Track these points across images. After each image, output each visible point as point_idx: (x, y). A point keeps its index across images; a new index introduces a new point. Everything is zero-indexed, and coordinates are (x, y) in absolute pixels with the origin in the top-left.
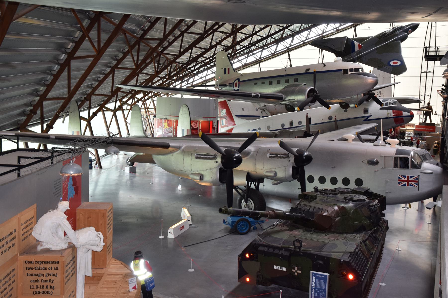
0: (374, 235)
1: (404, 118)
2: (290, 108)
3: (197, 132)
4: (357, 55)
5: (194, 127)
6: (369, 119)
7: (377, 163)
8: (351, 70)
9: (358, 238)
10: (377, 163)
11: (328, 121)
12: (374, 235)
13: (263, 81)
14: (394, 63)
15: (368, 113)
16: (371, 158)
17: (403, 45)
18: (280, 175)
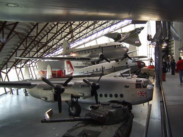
0: (126, 123)
2: (93, 63)
7: (129, 86)
8: (117, 45)
9: (119, 125)
10: (129, 86)
11: (112, 68)
12: (126, 123)
13: (82, 52)
16: (126, 85)
17: (139, 35)
18: (86, 94)
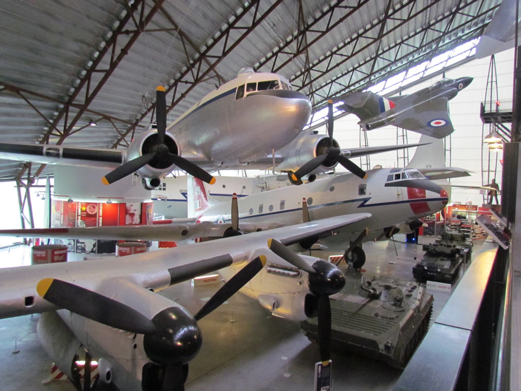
1: (429, 203)
3: (95, 221)
4: (388, 115)
5: (90, 213)
6: (367, 203)
8: (251, 86)
14: (436, 123)
17: (452, 104)
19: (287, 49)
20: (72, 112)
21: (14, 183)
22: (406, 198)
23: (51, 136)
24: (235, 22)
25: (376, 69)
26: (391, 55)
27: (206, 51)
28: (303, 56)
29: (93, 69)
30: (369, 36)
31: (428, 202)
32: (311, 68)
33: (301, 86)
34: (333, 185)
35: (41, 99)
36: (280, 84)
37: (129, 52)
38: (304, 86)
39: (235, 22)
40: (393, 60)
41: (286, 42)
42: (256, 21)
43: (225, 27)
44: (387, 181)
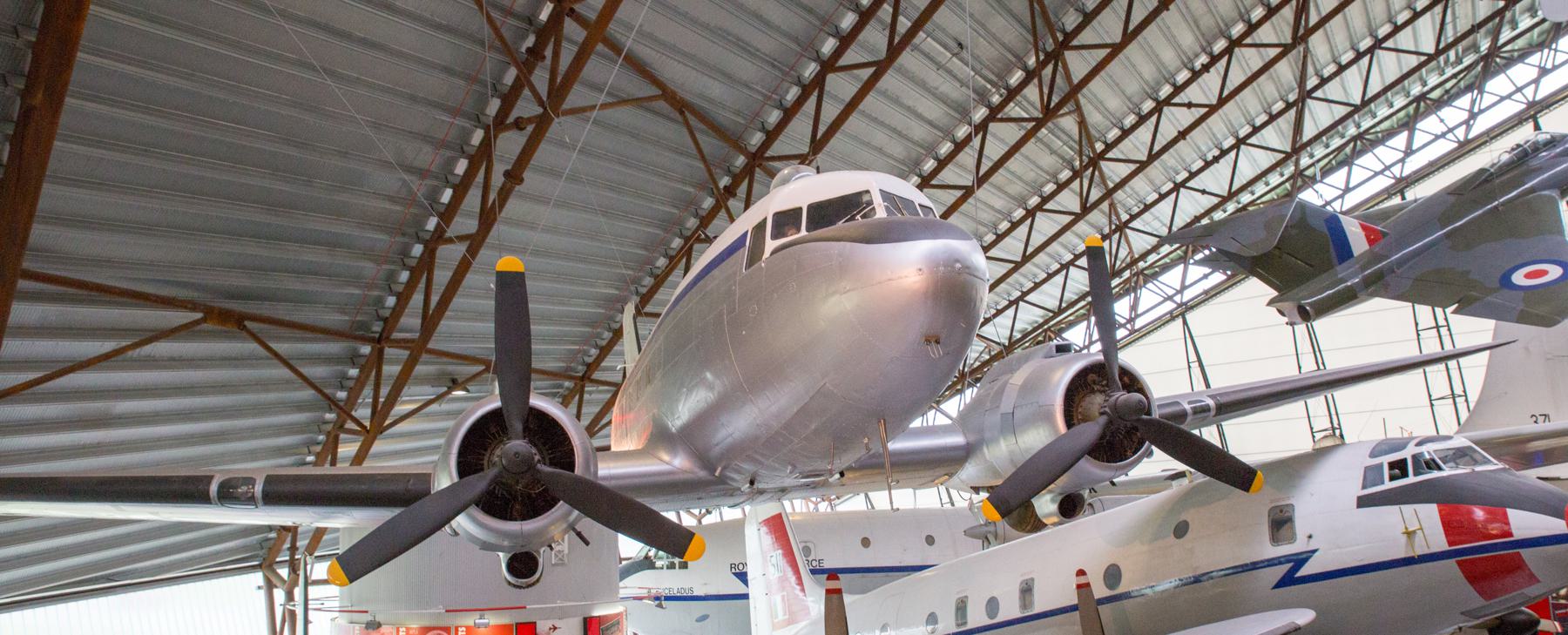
4: (1363, 269)
6: (1303, 572)
14: (1528, 276)
15: (1292, 538)
19: (1013, 110)
20: (392, 362)
21: (258, 578)
22: (1439, 542)
23: (342, 436)
24: (838, 53)
25: (1309, 132)
26: (1351, 86)
27: (766, 145)
28: (1068, 123)
29: (439, 237)
30: (1265, 41)
31: (1525, 553)
32: (1101, 156)
33: (1078, 210)
34: (1183, 517)
35: (310, 335)
36: (878, 200)
37: (526, 175)
38: (1086, 209)
39: (838, 53)
40: (1358, 101)
41: (1007, 88)
42: (897, 40)
43: (810, 70)
44: (1364, 487)
